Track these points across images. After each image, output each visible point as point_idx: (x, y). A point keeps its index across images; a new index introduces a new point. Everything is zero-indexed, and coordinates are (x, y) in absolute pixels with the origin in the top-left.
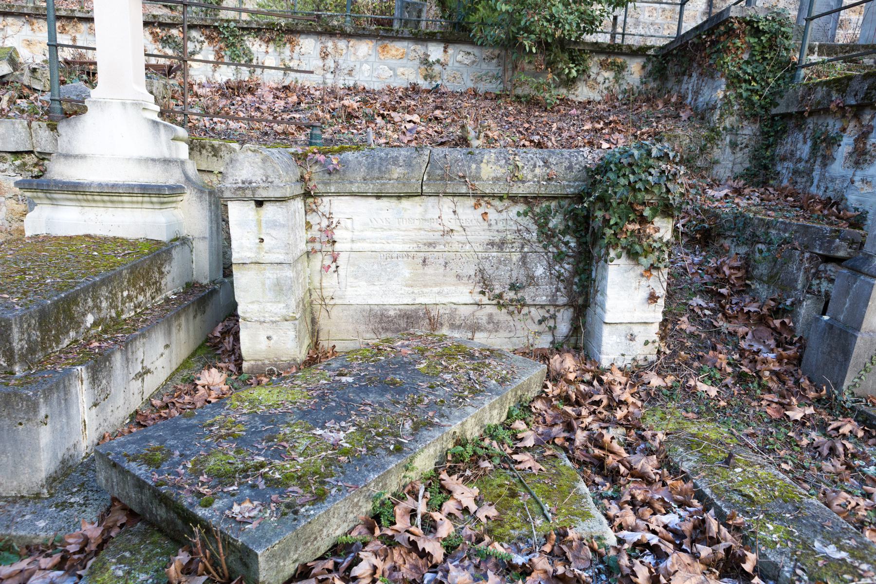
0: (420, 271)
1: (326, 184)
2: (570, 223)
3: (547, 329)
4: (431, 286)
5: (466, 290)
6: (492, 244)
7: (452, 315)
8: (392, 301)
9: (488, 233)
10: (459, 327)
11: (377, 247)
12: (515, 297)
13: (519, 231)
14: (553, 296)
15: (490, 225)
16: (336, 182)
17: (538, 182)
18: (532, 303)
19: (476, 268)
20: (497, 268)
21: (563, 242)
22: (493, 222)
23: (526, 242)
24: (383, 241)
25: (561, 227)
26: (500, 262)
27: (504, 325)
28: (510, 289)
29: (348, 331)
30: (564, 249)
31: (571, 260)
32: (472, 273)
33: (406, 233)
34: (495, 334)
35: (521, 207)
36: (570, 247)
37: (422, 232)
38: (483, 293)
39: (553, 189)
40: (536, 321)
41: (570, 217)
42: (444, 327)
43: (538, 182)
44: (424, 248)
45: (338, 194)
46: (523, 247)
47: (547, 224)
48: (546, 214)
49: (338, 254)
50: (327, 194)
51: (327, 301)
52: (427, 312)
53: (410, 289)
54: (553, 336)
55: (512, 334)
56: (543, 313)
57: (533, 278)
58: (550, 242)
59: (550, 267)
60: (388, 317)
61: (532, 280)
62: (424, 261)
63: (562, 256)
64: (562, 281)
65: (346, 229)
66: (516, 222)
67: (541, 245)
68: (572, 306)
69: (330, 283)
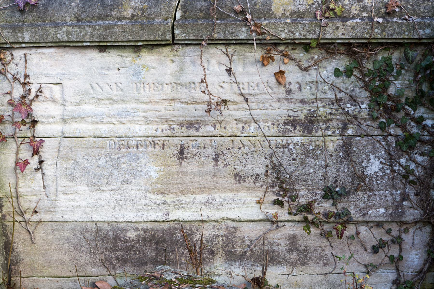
0: (176, 168)
1: (15, 28)
2: (425, 87)
3: (387, 260)
4: (194, 193)
5: (251, 198)
6: (293, 123)
7: (230, 237)
8: (131, 216)
9: (286, 105)
10: (241, 257)
11: (104, 129)
12: (333, 210)
13: (338, 100)
14: (397, 207)
15: (289, 92)
16: (32, 25)
17: (370, 18)
18: (361, 219)
19: (268, 162)
20: (302, 163)
21: (413, 119)
22: (294, 87)
23: (349, 119)
24: (113, 120)
25: (410, 94)
26: (307, 153)
27: (315, 254)
28: (324, 197)
29: (63, 263)
30: (415, 130)
31: (427, 148)
32: (261, 170)
33: (150, 106)
34: (301, 268)
35: (341, 62)
36: (424, 127)
37: (177, 105)
38: (279, 203)
39: (395, 31)
40: (369, 248)
41: (424, 78)
42: (217, 257)
43: (370, 18)
44: (179, 130)
45: (36, 45)
46: (344, 128)
47: (385, 89)
48: (384, 73)
49: (42, 141)
50: (19, 45)
51: (27, 216)
52: (187, 237)
53: (159, 197)
54: (398, 271)
55: (329, 269)
56: (379, 234)
57: (362, 177)
58: (391, 120)
59: (391, 160)
60: (126, 241)
61: (360, 181)
62: (181, 152)
63: (412, 141)
64: (412, 183)
65: (53, 100)
66: (333, 86)
67: (375, 124)
68: (429, 223)
69: (30, 187)
